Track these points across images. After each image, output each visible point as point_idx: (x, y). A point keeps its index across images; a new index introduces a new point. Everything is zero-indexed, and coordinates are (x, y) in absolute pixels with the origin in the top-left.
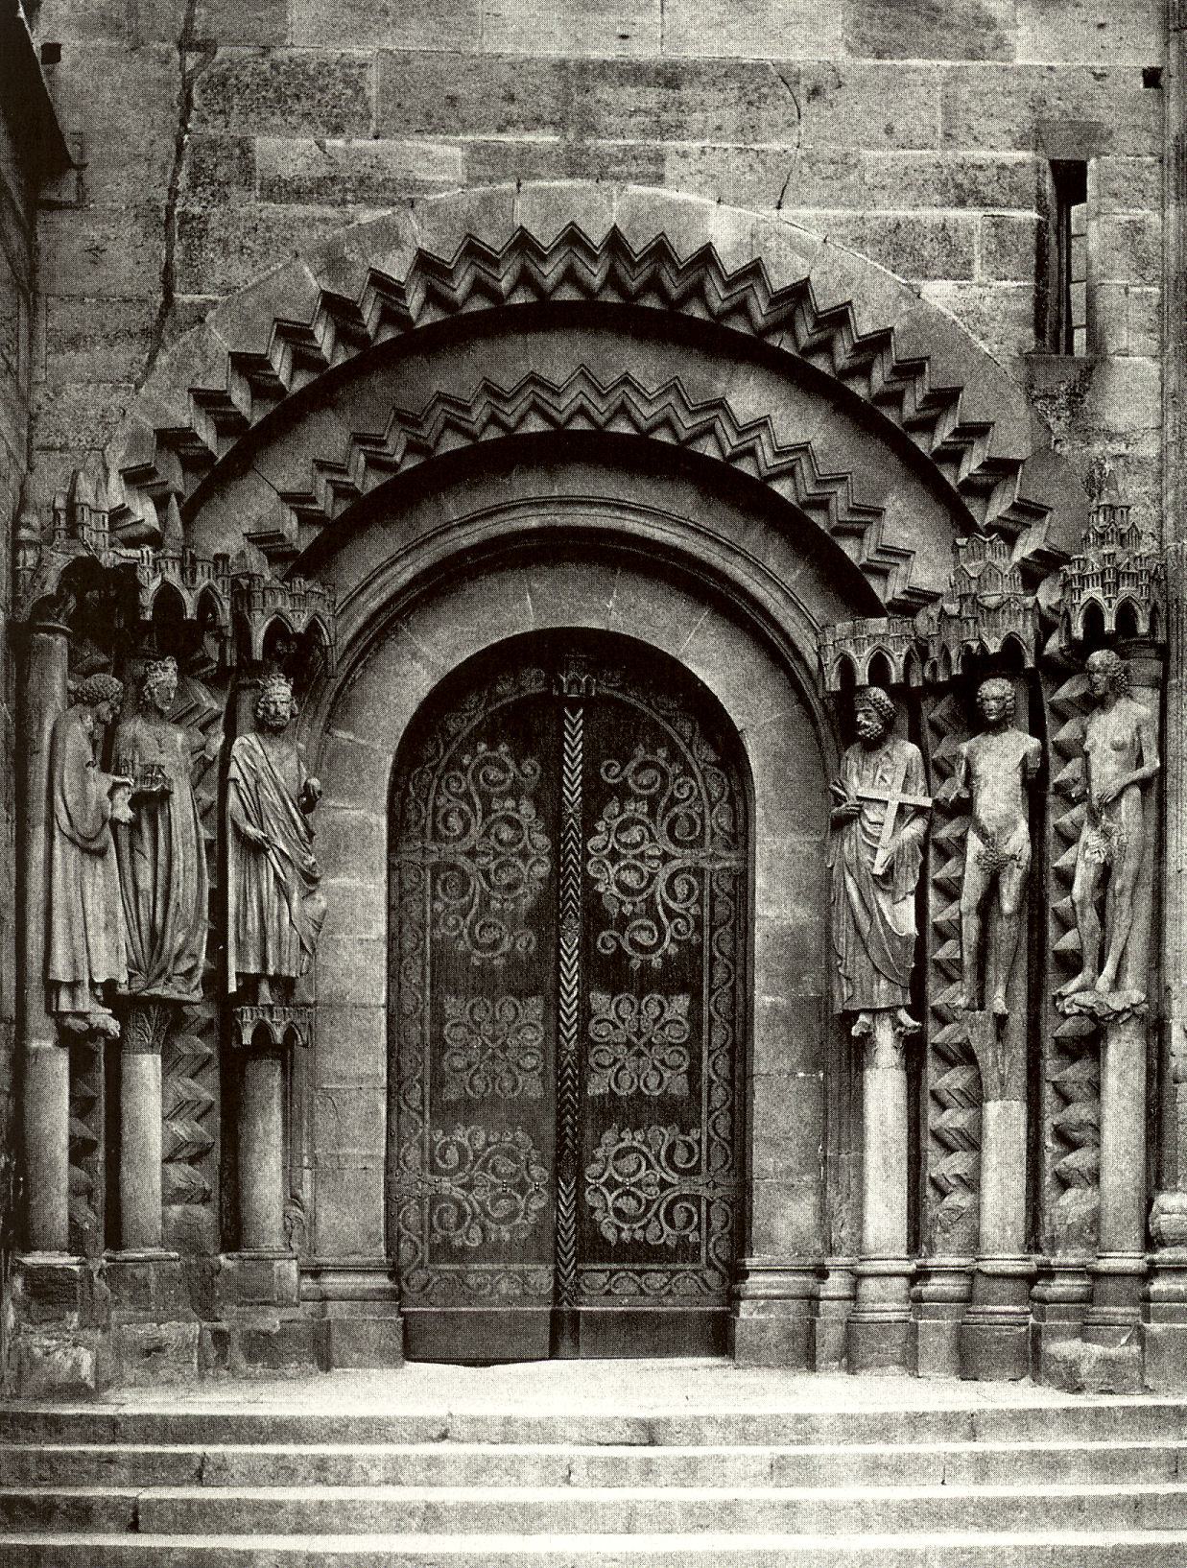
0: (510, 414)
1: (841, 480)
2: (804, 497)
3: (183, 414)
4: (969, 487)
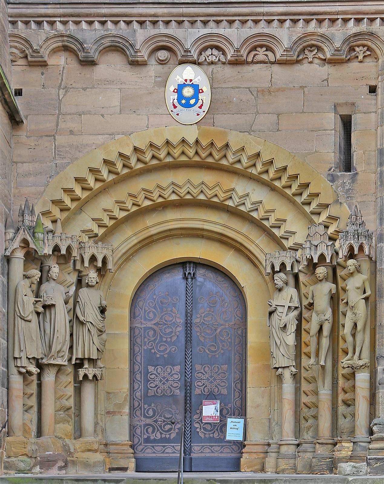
0: (166, 194)
1: (273, 211)
2: (261, 217)
3: (60, 195)
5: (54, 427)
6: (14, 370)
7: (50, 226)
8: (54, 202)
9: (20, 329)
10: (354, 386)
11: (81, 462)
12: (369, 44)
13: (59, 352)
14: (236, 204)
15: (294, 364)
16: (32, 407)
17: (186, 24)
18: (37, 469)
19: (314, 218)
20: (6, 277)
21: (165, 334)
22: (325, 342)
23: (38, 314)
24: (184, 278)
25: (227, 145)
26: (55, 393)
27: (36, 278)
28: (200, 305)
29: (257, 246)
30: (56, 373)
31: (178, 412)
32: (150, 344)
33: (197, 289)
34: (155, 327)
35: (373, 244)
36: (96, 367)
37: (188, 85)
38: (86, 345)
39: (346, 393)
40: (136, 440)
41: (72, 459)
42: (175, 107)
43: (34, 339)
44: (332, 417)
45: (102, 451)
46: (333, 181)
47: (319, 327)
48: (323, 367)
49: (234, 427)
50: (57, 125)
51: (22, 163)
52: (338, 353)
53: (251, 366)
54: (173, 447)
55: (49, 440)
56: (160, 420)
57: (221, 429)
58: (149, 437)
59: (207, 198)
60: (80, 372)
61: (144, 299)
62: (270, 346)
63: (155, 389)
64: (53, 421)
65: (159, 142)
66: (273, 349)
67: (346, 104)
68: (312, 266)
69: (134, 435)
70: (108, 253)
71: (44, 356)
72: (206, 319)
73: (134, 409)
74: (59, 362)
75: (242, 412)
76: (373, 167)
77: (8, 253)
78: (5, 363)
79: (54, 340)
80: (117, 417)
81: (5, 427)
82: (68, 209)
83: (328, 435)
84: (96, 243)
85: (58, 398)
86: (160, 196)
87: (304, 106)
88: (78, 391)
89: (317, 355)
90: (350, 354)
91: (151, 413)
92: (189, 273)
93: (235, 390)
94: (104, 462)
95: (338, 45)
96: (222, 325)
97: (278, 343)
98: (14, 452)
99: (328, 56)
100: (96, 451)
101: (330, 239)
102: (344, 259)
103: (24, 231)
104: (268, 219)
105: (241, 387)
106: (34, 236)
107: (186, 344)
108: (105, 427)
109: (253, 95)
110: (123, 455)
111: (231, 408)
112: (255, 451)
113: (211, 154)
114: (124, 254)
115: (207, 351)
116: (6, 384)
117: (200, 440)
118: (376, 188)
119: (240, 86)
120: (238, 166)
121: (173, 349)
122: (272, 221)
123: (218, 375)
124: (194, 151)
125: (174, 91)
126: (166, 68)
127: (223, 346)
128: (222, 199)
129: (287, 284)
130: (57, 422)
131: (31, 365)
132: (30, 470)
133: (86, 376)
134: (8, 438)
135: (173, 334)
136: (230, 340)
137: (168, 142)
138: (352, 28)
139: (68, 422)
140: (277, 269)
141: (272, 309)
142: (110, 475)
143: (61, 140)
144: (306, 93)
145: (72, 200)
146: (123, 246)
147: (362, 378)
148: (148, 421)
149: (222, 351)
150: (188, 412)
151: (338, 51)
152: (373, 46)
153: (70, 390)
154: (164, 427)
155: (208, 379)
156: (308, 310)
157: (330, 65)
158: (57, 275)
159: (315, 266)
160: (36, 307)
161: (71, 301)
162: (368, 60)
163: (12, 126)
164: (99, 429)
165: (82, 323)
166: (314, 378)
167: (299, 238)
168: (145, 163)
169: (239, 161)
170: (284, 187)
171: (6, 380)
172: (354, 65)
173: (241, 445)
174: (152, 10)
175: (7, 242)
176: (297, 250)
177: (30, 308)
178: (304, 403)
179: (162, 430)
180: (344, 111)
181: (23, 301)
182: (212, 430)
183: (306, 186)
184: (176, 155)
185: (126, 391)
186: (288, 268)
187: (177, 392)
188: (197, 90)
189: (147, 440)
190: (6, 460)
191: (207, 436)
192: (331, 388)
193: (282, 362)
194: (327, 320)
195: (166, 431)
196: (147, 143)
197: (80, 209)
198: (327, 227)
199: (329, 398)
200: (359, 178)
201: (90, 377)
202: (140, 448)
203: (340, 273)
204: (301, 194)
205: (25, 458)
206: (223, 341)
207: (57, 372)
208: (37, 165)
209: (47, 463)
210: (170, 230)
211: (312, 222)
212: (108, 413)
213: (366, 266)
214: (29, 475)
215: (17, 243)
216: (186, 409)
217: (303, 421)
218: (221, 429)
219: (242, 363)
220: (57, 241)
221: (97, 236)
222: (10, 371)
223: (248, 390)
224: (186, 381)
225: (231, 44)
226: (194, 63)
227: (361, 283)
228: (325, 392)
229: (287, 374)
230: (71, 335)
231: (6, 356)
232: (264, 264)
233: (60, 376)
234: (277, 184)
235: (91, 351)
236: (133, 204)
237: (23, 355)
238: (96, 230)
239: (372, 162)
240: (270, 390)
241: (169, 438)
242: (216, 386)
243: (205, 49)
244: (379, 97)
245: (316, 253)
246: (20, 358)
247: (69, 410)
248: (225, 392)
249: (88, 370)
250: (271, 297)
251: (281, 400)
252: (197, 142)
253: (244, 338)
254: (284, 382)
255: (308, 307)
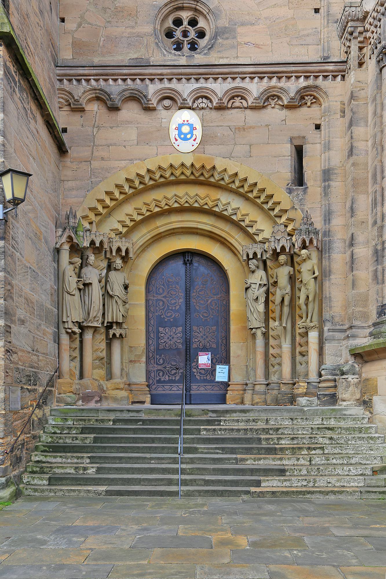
0: (171, 203)
1: (247, 215)
2: (239, 219)
4: (276, 216)
5: (92, 372)
6: (63, 331)
7: (88, 226)
8: (90, 209)
9: (67, 301)
10: (307, 342)
11: (112, 397)
12: (315, 94)
13: (95, 317)
14: (221, 210)
15: (264, 326)
16: (76, 357)
17: (184, 80)
18: (80, 402)
19: (277, 220)
20: (57, 263)
21: (171, 304)
22: (286, 310)
23: (80, 290)
24: (184, 264)
25: (214, 168)
26: (92, 347)
27: (78, 264)
28: (196, 283)
29: (236, 240)
30: (92, 334)
31: (181, 360)
32: (160, 312)
33: (194, 271)
34: (163, 299)
35: (320, 239)
36: (122, 328)
37: (186, 124)
38: (114, 312)
39: (302, 346)
40: (151, 381)
41: (105, 395)
42: (176, 140)
43: (77, 308)
44: (292, 364)
45: (127, 389)
46: (290, 193)
47: (282, 298)
48: (285, 328)
49: (222, 371)
50: (92, 154)
51: (68, 181)
52: (295, 318)
53: (233, 327)
54: (178, 386)
55: (89, 382)
56: (168, 366)
57: (212, 373)
58: (160, 379)
59: (200, 205)
60: (110, 332)
61: (156, 279)
62: (246, 313)
63: (164, 344)
64: (91, 367)
65: (165, 166)
66: (249, 314)
67: (299, 137)
68: (276, 254)
69: (149, 378)
70: (130, 246)
71: (84, 321)
72: (200, 293)
73: (149, 359)
74: (95, 324)
75: (226, 360)
76: (319, 183)
77: (58, 246)
78: (56, 325)
79: (92, 309)
80: (137, 364)
81: (57, 372)
82: (101, 214)
83: (289, 377)
84: (121, 238)
85: (94, 351)
86: (166, 204)
87: (268, 139)
88: (109, 345)
89: (281, 319)
90: (304, 319)
91: (161, 361)
92: (188, 260)
93: (221, 345)
94: (128, 397)
95: (292, 95)
96: (212, 298)
97: (252, 310)
98: (63, 390)
99: (286, 103)
100: (122, 389)
101: (289, 235)
102: (299, 249)
103: (69, 230)
104: (244, 221)
105: (226, 342)
106: (76, 234)
107: (186, 311)
108: (129, 372)
109: (232, 131)
110: (141, 392)
111: (219, 358)
112: (237, 389)
113: (202, 174)
114: (141, 246)
115: (201, 316)
116: (57, 340)
117: (197, 381)
118: (321, 198)
119: (223, 125)
120: (222, 182)
121: (177, 315)
122: (247, 222)
123: (210, 334)
124: (191, 172)
125: (175, 129)
126: (169, 112)
127: (213, 313)
128: (211, 206)
129: (258, 267)
130: (94, 368)
131: (75, 327)
132: (75, 403)
133: (114, 335)
134: (59, 380)
135: (177, 304)
136: (217, 309)
137: (171, 166)
138: (302, 83)
139: (102, 368)
140: (251, 256)
141: (248, 285)
142: (132, 406)
143: (95, 164)
144: (270, 129)
145: (104, 207)
146: (140, 240)
147: (313, 335)
148: (160, 367)
149: (212, 317)
150: (188, 361)
151: (293, 99)
152: (318, 96)
153: (103, 345)
154: (171, 372)
155: (202, 337)
156: (273, 287)
157: (287, 110)
158: (93, 261)
159: (278, 254)
160: (78, 285)
161: (103, 280)
162: (314, 105)
163: (60, 154)
164: (124, 374)
165: (111, 297)
166: (278, 336)
167: (266, 234)
168: (155, 180)
169: (223, 179)
170: (255, 198)
171: (57, 338)
172: (304, 109)
173: (226, 385)
174: (159, 71)
175: (57, 238)
176: (265, 243)
177: (74, 285)
178: (271, 354)
179: (169, 374)
180: (298, 143)
181: (69, 280)
182: (205, 374)
183: (271, 196)
184: (177, 175)
185: (143, 345)
186: (259, 256)
187: (180, 346)
188: (193, 128)
189: (159, 381)
190: (57, 396)
191: (202, 378)
192: (290, 343)
193: (256, 324)
194: (287, 293)
195: (173, 375)
196: (157, 166)
197: (109, 214)
198: (286, 226)
199: (290, 350)
200: (309, 190)
201: (118, 335)
202: (154, 387)
203: (296, 259)
204: (267, 203)
205: (71, 394)
206: (212, 309)
207: (94, 332)
208: (78, 182)
209: (87, 398)
210: (174, 229)
211: (275, 223)
212: (131, 361)
213: (314, 255)
214: (74, 407)
215: (64, 239)
216: (186, 359)
217: (271, 367)
218: (212, 373)
219: (226, 325)
220: (93, 237)
221: (122, 233)
222: (60, 331)
223: (231, 344)
224: (186, 338)
225: (216, 95)
226: (190, 108)
227: (312, 266)
228: (287, 346)
229: (259, 333)
230: (104, 305)
231: (57, 320)
232: (241, 253)
233: (96, 335)
234: (250, 195)
235: (118, 317)
236: (147, 210)
237: (69, 319)
238: (121, 229)
239: (318, 179)
240: (247, 344)
241: (175, 379)
242: (208, 342)
243: (197, 98)
244: (323, 132)
245: (279, 245)
246: (67, 322)
247: (103, 360)
248: (214, 346)
249: (117, 331)
250: (246, 277)
251: (255, 352)
252: (192, 165)
253: (228, 307)
254: (257, 338)
255: (273, 284)
